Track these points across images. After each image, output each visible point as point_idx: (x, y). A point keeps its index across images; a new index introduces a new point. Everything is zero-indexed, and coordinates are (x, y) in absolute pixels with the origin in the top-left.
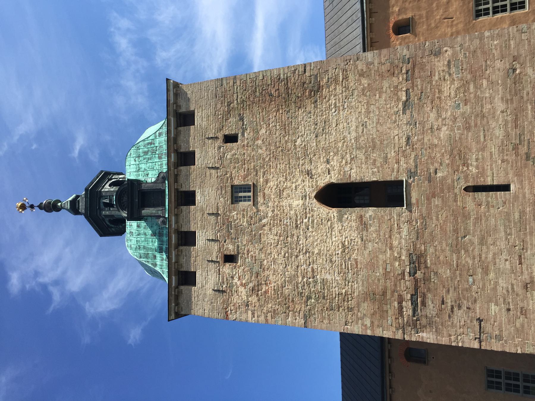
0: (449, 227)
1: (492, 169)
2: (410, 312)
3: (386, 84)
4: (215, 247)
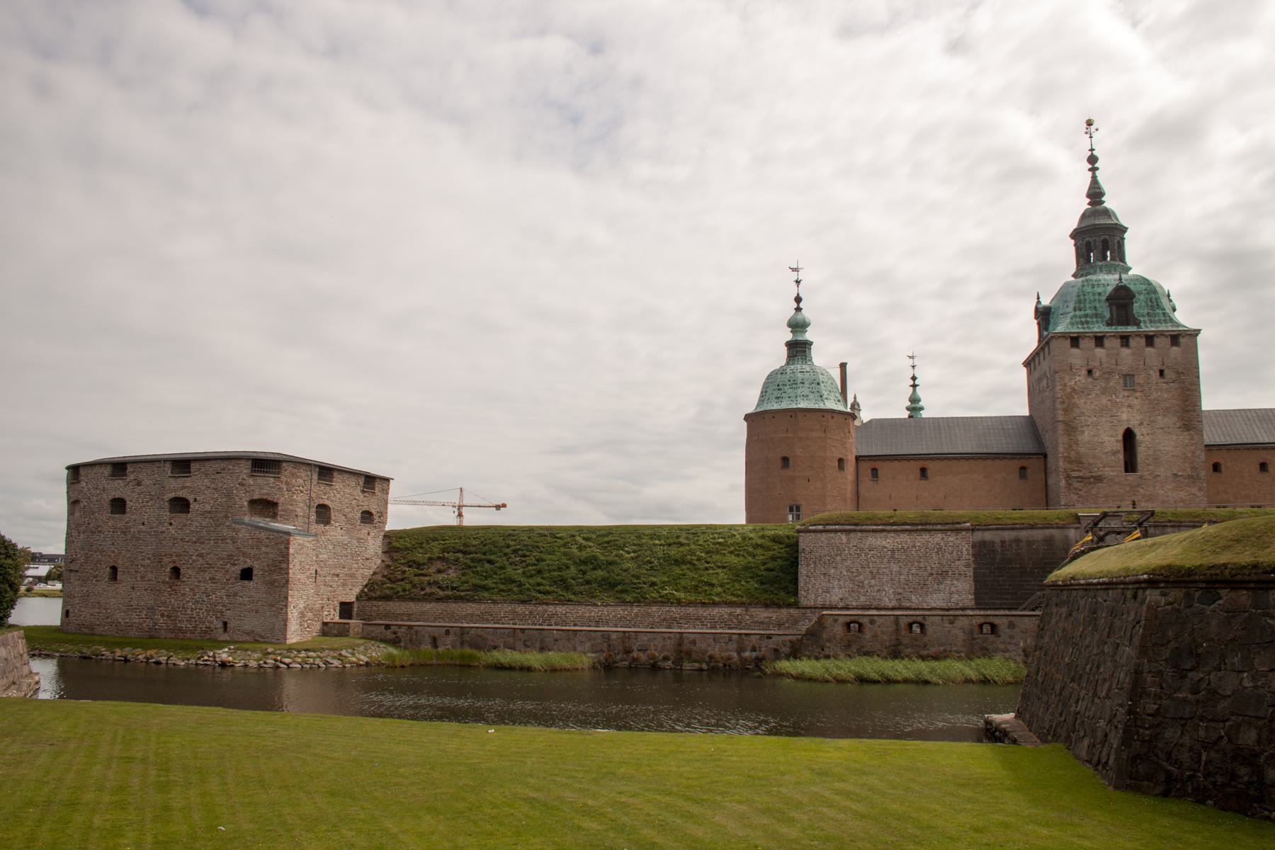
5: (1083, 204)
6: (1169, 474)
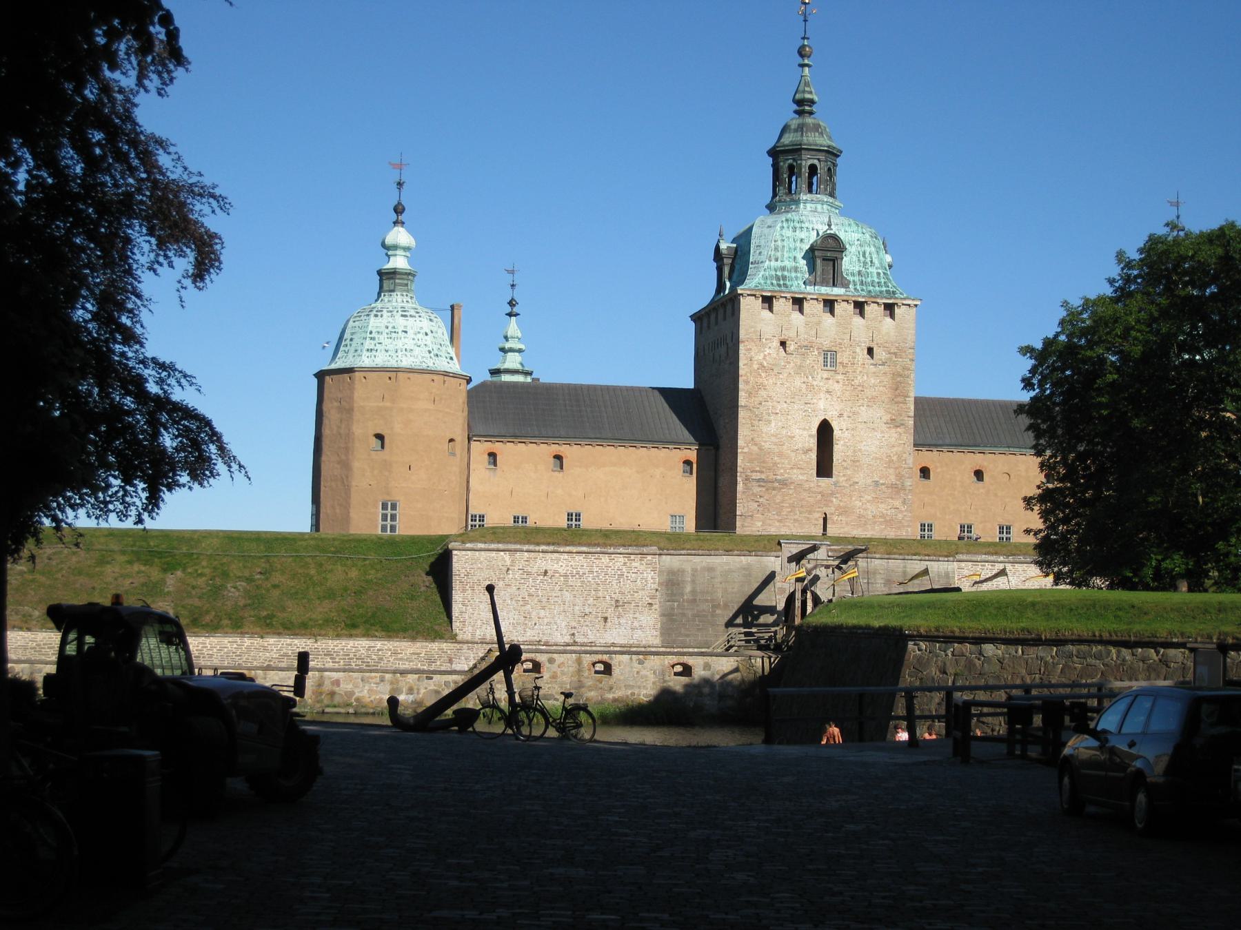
0: (804, 503)
3: (891, 471)
5: (787, 113)
6: (869, 481)
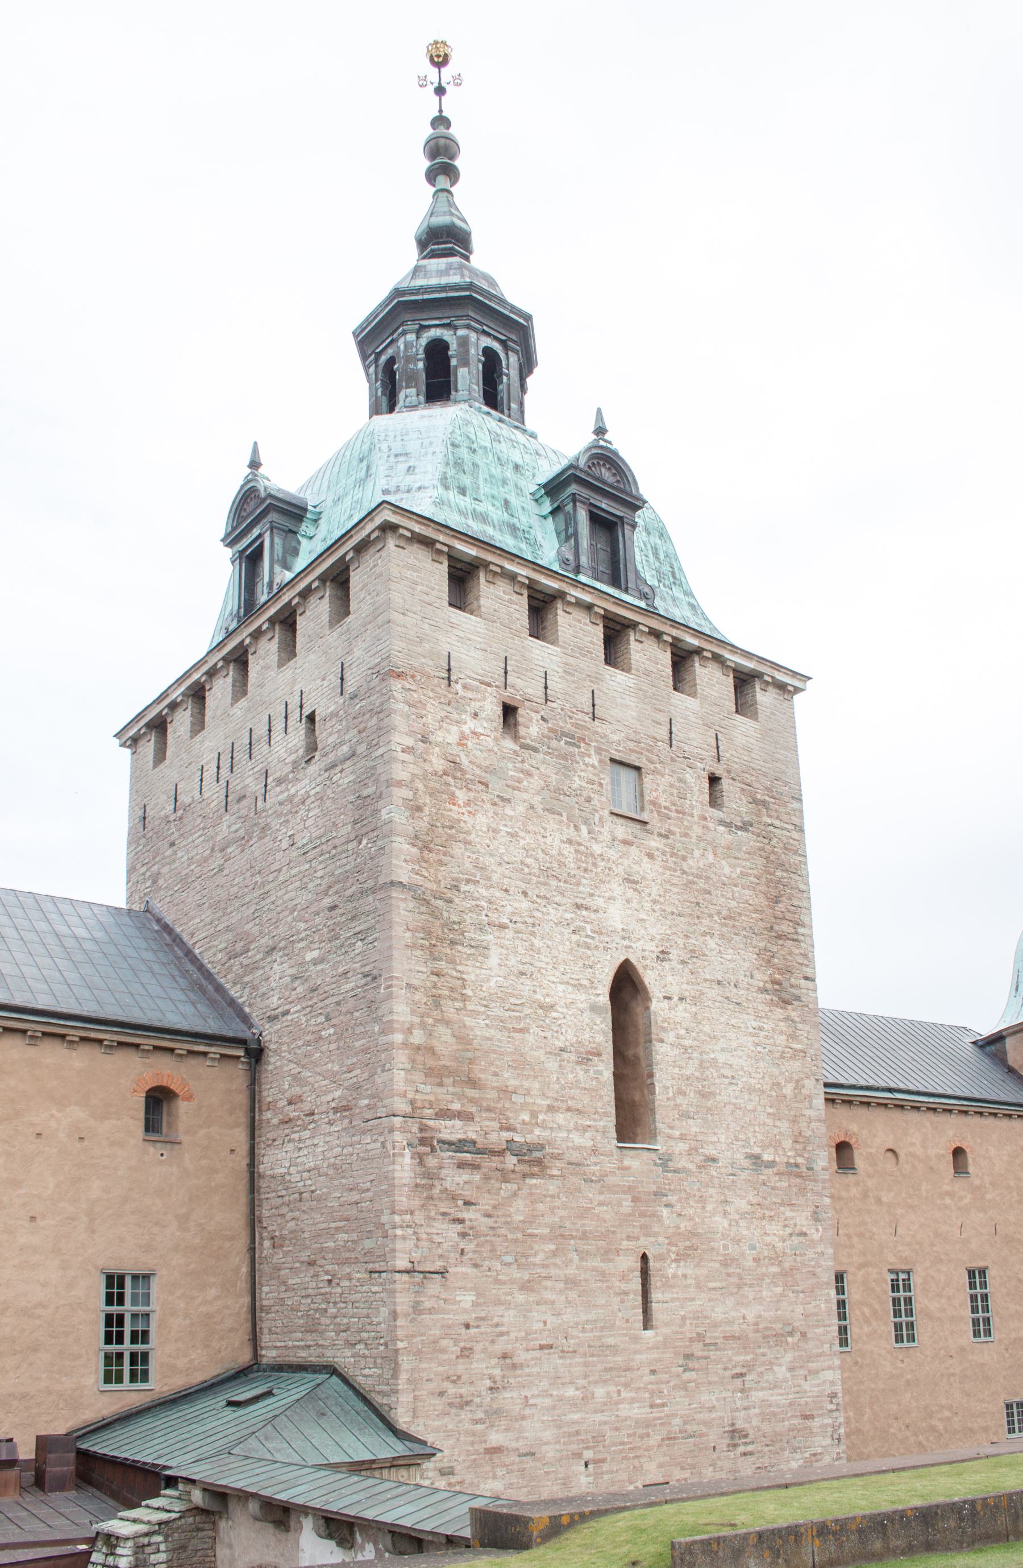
0: (590, 1225)
1: (673, 1300)
2: (445, 1136)
4: (536, 691)
